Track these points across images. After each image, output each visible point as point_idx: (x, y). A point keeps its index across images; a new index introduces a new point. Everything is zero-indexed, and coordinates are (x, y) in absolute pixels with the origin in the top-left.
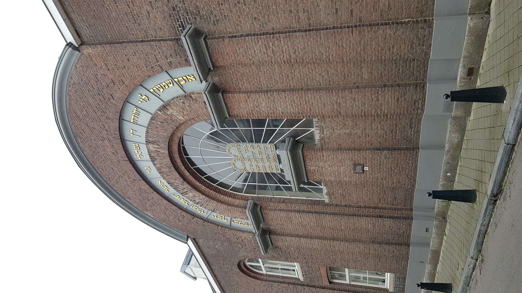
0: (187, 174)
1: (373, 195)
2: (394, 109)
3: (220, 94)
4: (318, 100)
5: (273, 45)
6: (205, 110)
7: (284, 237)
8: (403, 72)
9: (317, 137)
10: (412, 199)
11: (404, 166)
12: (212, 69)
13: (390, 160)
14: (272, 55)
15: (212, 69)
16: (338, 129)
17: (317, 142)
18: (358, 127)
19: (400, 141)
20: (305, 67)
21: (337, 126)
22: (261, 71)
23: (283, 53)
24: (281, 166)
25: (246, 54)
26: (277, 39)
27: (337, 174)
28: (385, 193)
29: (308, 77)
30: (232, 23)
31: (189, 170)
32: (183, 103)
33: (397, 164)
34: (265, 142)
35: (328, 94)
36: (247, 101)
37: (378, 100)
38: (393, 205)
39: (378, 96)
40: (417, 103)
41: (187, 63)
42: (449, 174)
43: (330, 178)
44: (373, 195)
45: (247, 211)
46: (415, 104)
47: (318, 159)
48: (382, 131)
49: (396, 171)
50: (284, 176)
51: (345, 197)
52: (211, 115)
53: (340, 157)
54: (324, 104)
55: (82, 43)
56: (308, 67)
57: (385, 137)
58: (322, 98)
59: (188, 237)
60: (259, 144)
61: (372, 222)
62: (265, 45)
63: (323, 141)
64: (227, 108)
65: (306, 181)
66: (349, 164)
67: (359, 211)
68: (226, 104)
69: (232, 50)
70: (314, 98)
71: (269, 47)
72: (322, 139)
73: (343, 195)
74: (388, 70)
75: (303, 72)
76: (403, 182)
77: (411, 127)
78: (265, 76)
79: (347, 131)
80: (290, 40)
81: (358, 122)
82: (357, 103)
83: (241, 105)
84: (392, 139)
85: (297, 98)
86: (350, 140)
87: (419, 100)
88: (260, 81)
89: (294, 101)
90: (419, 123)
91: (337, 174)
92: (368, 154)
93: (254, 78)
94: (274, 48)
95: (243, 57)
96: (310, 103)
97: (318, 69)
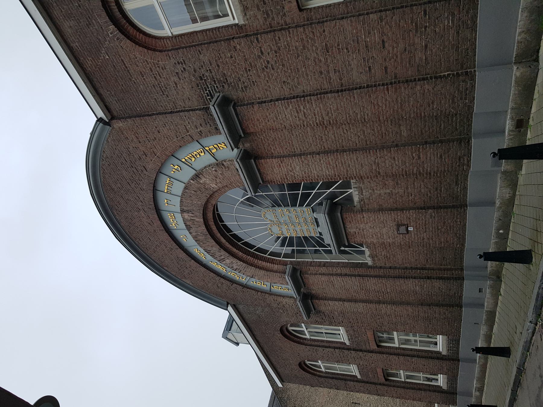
0: (223, 240)
1: (419, 255)
2: (437, 167)
3: (253, 160)
4: (354, 161)
5: (304, 108)
6: (238, 177)
7: (326, 301)
8: (445, 128)
9: (356, 199)
10: (462, 258)
11: (452, 224)
12: (243, 136)
13: (436, 219)
14: (304, 118)
15: (243, 136)
16: (378, 189)
17: (356, 204)
18: (399, 186)
19: (446, 198)
20: (339, 128)
21: (377, 186)
22: (293, 135)
23: (315, 115)
24: (319, 230)
25: (277, 119)
26: (308, 102)
27: (379, 235)
28: (432, 253)
29: (343, 138)
30: (261, 89)
32: (216, 171)
33: (444, 223)
34: (301, 205)
35: (365, 154)
36: (280, 165)
37: (419, 158)
38: (441, 265)
39: (419, 153)
40: (462, 159)
41: (217, 131)
42: (501, 231)
43: (372, 240)
44: (419, 255)
45: (286, 277)
46: (460, 160)
48: (426, 190)
49: (443, 230)
50: (322, 239)
51: (389, 258)
52: (245, 182)
53: (382, 218)
54: (362, 165)
55: (113, 118)
56: (343, 128)
57: (429, 195)
58: (359, 159)
60: (295, 208)
61: (420, 284)
62: (296, 108)
63: (362, 203)
64: (260, 174)
65: (347, 244)
66: (392, 225)
67: (404, 273)
68: (259, 170)
69: (262, 116)
70: (351, 159)
71: (300, 110)
72: (361, 200)
73: (387, 257)
74: (429, 126)
75: (337, 133)
76: (452, 242)
77: (457, 184)
78: (297, 140)
79: (388, 191)
80: (322, 102)
81: (399, 181)
82: (397, 162)
83: (275, 170)
84: (437, 197)
85: (332, 160)
86: (391, 200)
87: (464, 155)
88: (293, 145)
89: (329, 163)
90: (466, 179)
92: (412, 214)
93: (286, 142)
94: (305, 111)
95: (274, 122)
96: (347, 164)
97: (353, 129)
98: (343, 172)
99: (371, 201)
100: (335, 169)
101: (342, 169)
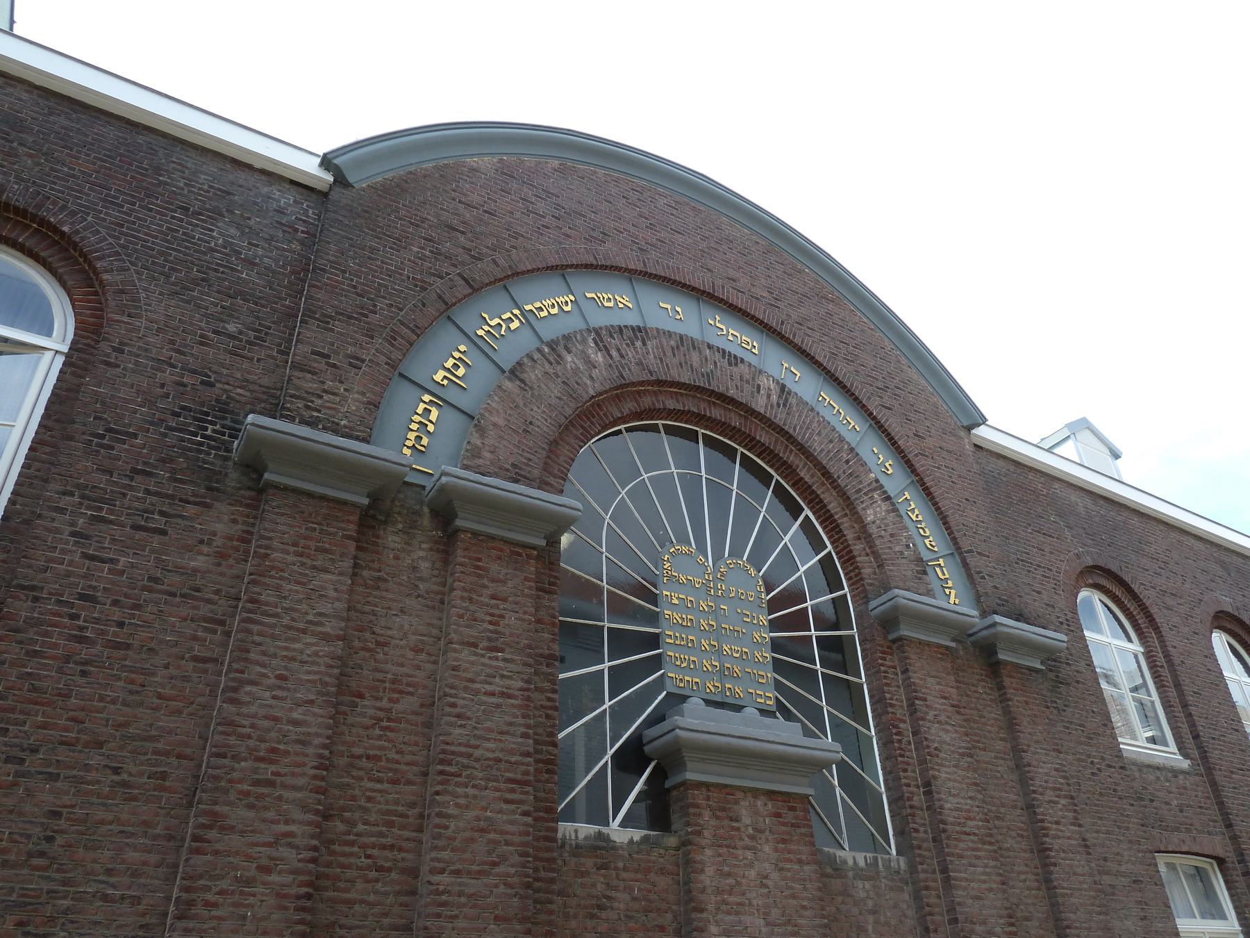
4: (985, 882)
7: (347, 564)
27: (732, 899)
31: (671, 414)
35: (1005, 912)
36: (945, 698)
43: (710, 871)
47: (784, 841)
51: (592, 916)
59: (341, 180)
73: (601, 908)
85: (978, 827)
89: (970, 819)
91: (732, 899)
96: (976, 862)
98: (956, 846)
99: (840, 899)
100: (958, 828)
101: (961, 845)
